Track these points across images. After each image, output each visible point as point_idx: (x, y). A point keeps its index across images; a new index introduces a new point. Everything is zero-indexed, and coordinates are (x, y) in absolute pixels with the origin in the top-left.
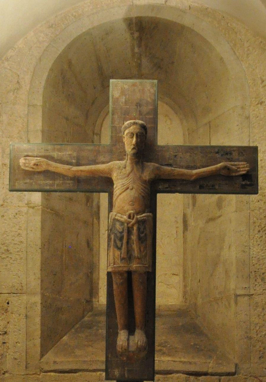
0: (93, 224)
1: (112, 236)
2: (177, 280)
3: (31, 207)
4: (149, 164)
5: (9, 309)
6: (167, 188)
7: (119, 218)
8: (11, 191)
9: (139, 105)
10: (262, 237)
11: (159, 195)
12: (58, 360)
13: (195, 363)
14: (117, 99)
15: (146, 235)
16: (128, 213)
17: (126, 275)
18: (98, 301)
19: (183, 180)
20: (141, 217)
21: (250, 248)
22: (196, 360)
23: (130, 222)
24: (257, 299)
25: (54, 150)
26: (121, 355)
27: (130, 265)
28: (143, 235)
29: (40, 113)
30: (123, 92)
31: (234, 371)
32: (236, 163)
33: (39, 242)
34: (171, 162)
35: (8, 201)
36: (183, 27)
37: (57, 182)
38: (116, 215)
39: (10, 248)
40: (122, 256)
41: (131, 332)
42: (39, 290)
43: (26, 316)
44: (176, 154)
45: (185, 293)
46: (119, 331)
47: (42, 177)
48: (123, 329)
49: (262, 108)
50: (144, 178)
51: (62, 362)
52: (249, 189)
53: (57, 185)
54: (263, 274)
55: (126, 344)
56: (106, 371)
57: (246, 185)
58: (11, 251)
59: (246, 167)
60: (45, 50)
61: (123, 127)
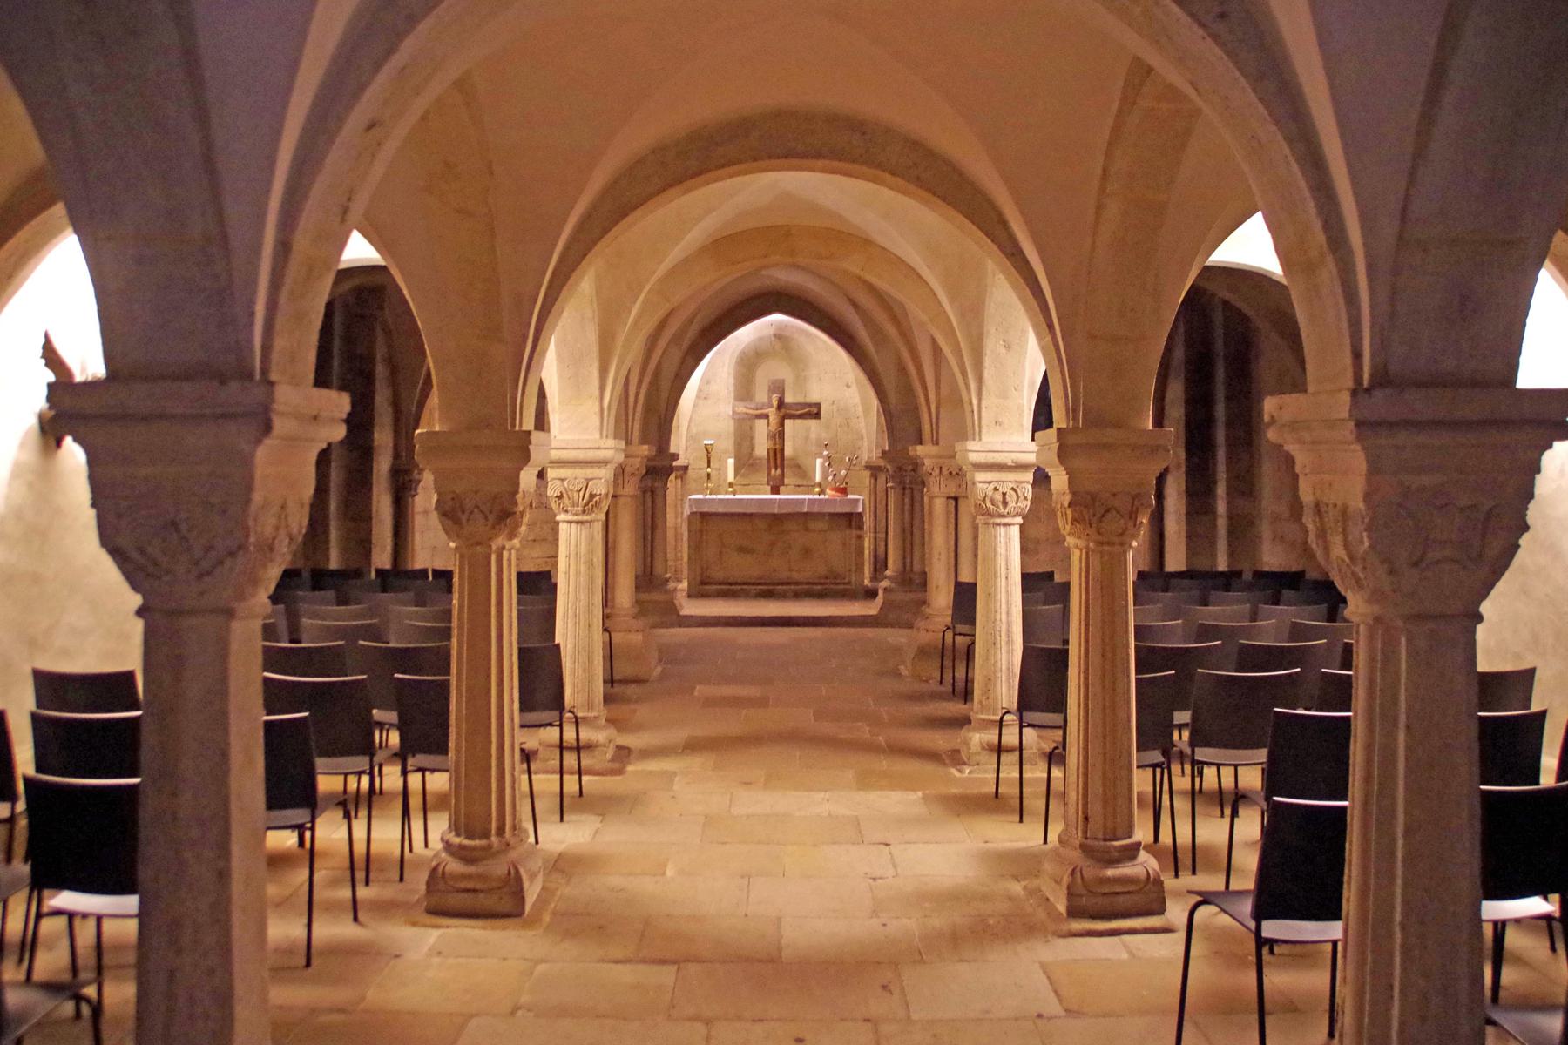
41: (776, 469)
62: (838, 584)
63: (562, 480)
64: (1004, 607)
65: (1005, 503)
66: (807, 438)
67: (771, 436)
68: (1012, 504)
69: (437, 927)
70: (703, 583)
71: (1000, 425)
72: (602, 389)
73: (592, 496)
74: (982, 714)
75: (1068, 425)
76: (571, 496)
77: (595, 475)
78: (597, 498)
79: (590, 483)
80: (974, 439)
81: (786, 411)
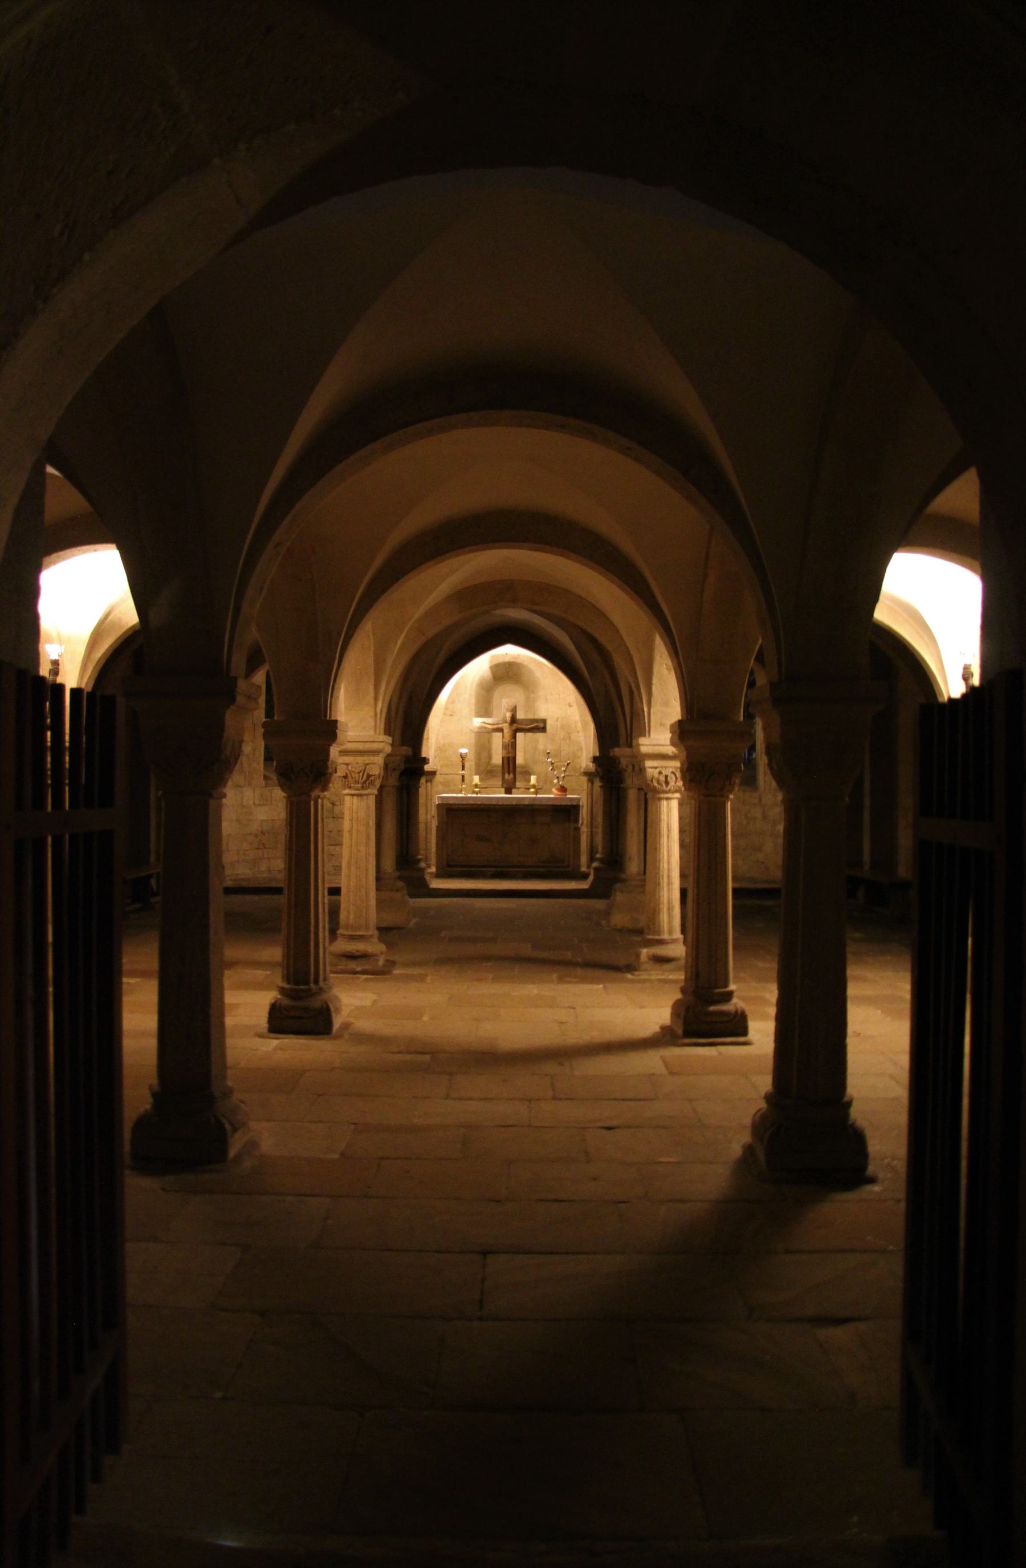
30: (507, 703)
41: (509, 774)
62: (559, 867)
63: (347, 765)
64: (666, 858)
65: (667, 783)
66: (536, 749)
67: (505, 747)
68: (672, 784)
69: (277, 1038)
70: (449, 866)
71: (664, 726)
72: (376, 699)
73: (369, 776)
74: (649, 935)
75: (687, 718)
76: (353, 776)
77: (371, 762)
78: (372, 778)
79: (367, 767)
80: (645, 736)
81: (517, 725)
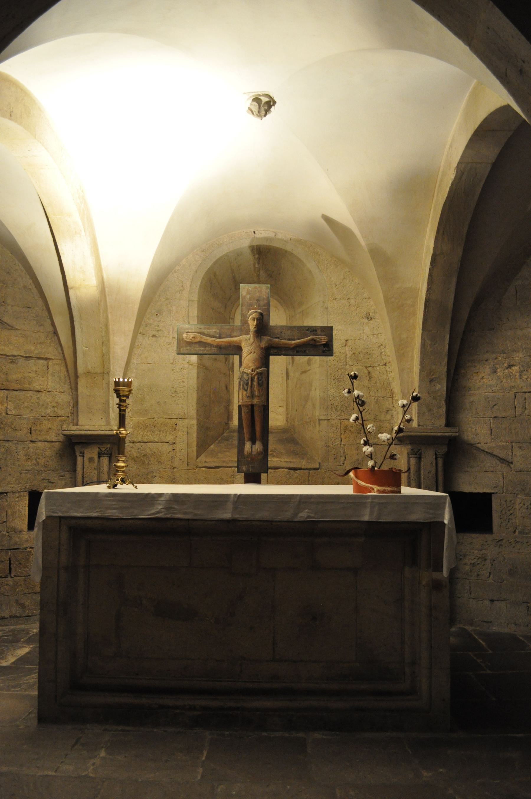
0: (229, 375)
1: (242, 383)
2: (282, 410)
3: (190, 364)
4: (265, 337)
5: (177, 428)
6: (276, 352)
7: (246, 371)
8: (178, 354)
9: (258, 300)
10: (336, 383)
11: (271, 357)
12: (207, 460)
13: (294, 462)
14: (245, 296)
15: (263, 382)
16: (251, 368)
17: (250, 407)
18: (233, 423)
19: (286, 347)
20: (259, 371)
21: (328, 390)
22: (294, 460)
23: (252, 374)
24: (333, 422)
25: (205, 328)
26: (247, 457)
27: (253, 401)
28: (261, 382)
29: (196, 306)
30: (248, 292)
31: (318, 467)
32: (319, 337)
33: (195, 386)
34: (278, 336)
35: (176, 360)
36: (286, 251)
37: (207, 349)
38: (244, 370)
39: (177, 390)
40: (248, 395)
41: (253, 443)
42: (195, 416)
43: (188, 433)
44: (282, 331)
45: (287, 418)
46: (246, 442)
47: (197, 345)
48: (248, 441)
49: (336, 302)
50: (262, 346)
51: (210, 462)
52: (328, 353)
53: (207, 350)
54: (336, 406)
55: (250, 450)
56: (238, 467)
57: (326, 350)
58: (178, 392)
59: (326, 339)
60: (199, 266)
61: (248, 314)
